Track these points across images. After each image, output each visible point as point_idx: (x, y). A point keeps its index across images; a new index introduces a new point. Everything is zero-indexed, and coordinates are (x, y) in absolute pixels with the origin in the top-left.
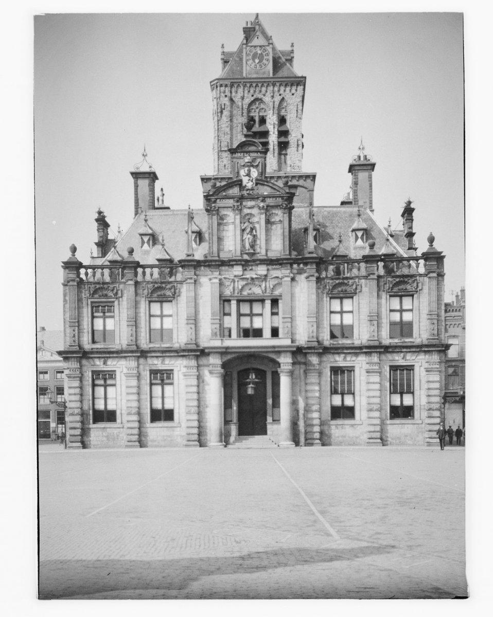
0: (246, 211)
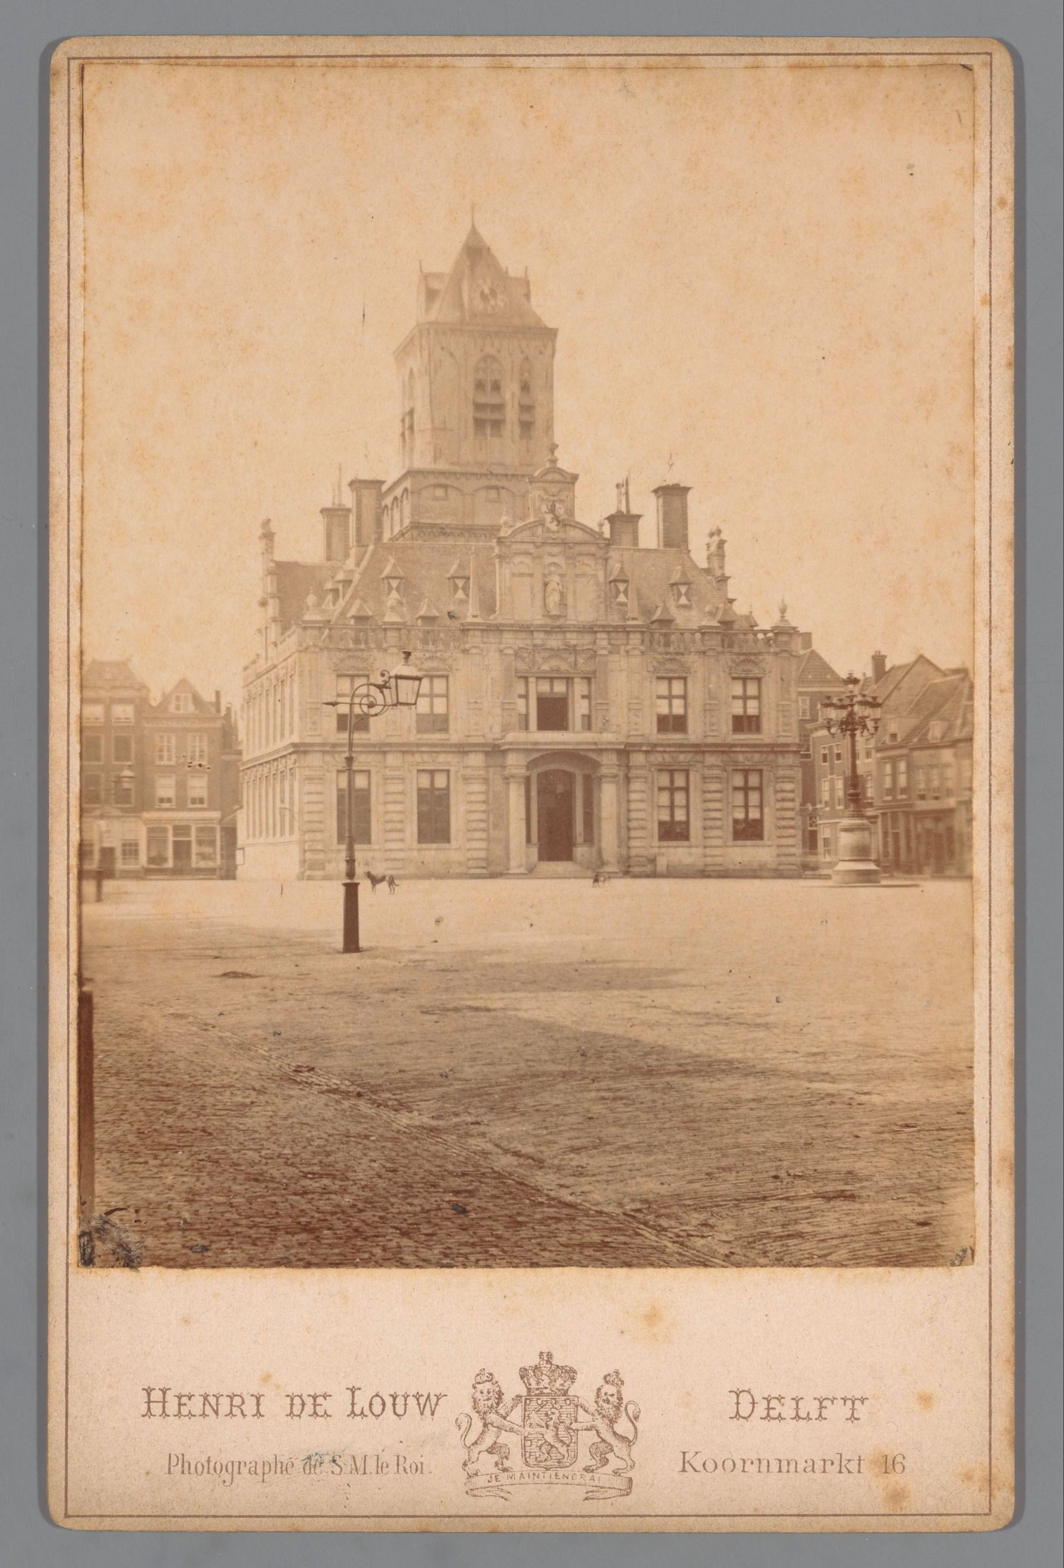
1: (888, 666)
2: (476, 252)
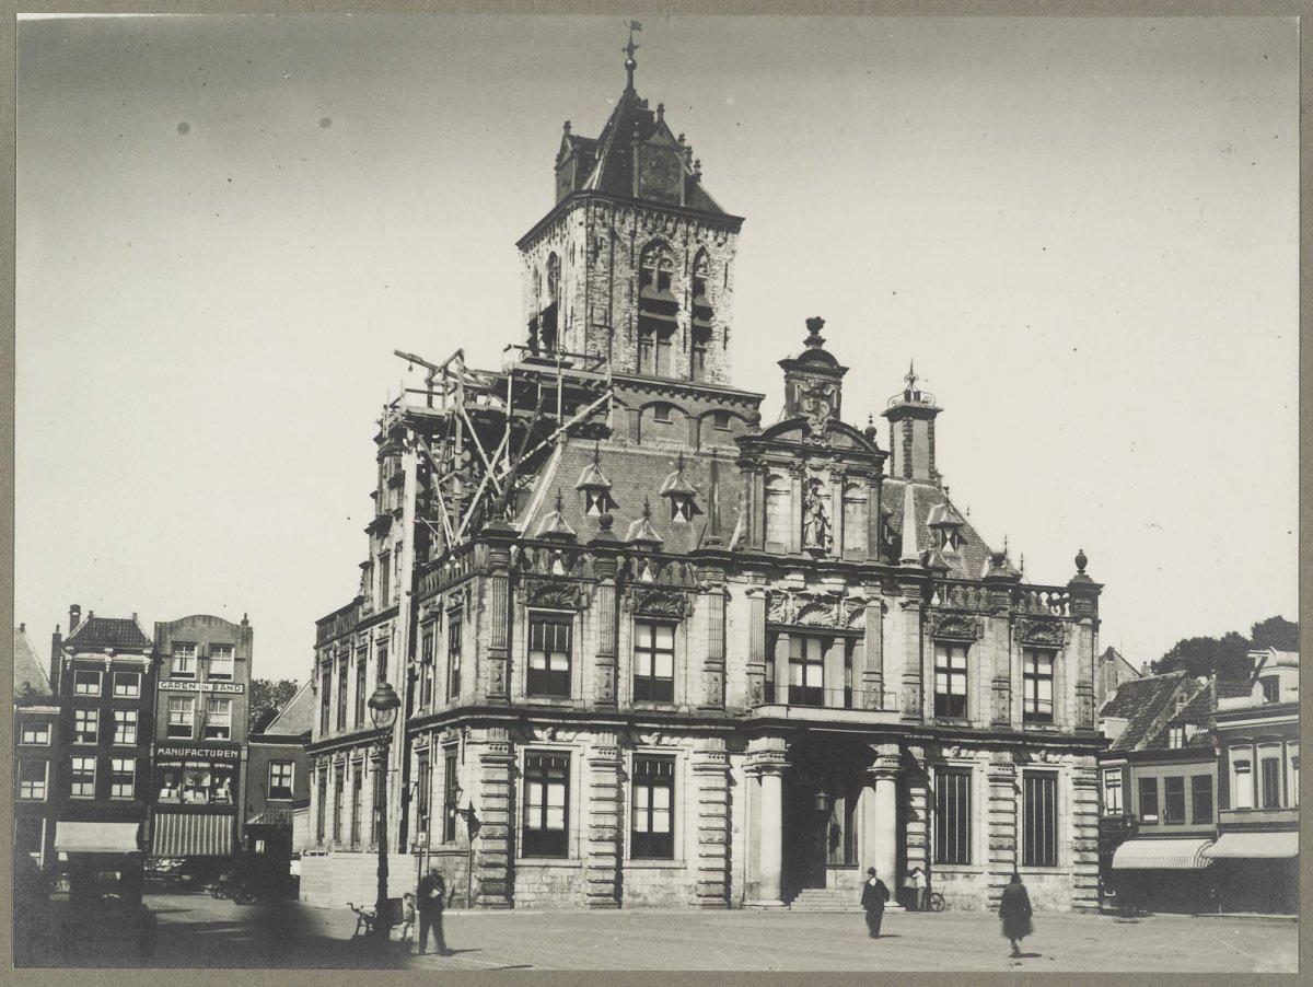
0: (810, 474)
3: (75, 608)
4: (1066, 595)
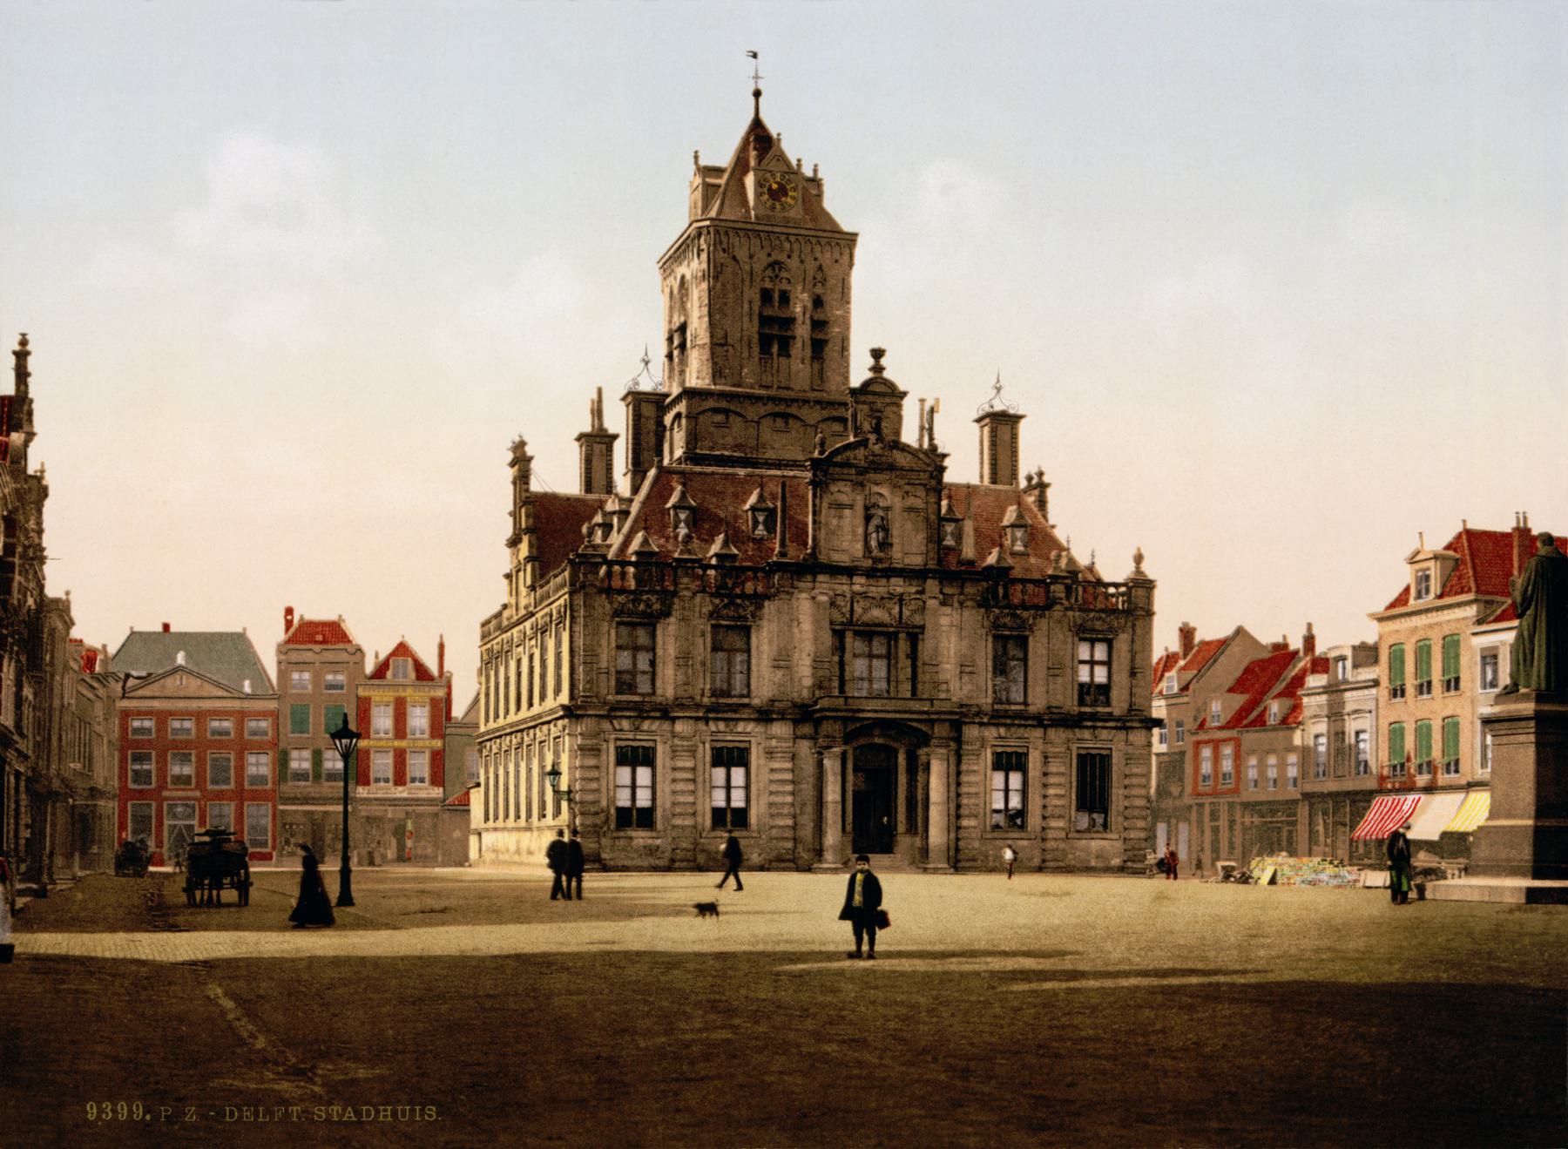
1: (1198, 638)
2: (760, 138)
3: (289, 611)
4: (1123, 589)
